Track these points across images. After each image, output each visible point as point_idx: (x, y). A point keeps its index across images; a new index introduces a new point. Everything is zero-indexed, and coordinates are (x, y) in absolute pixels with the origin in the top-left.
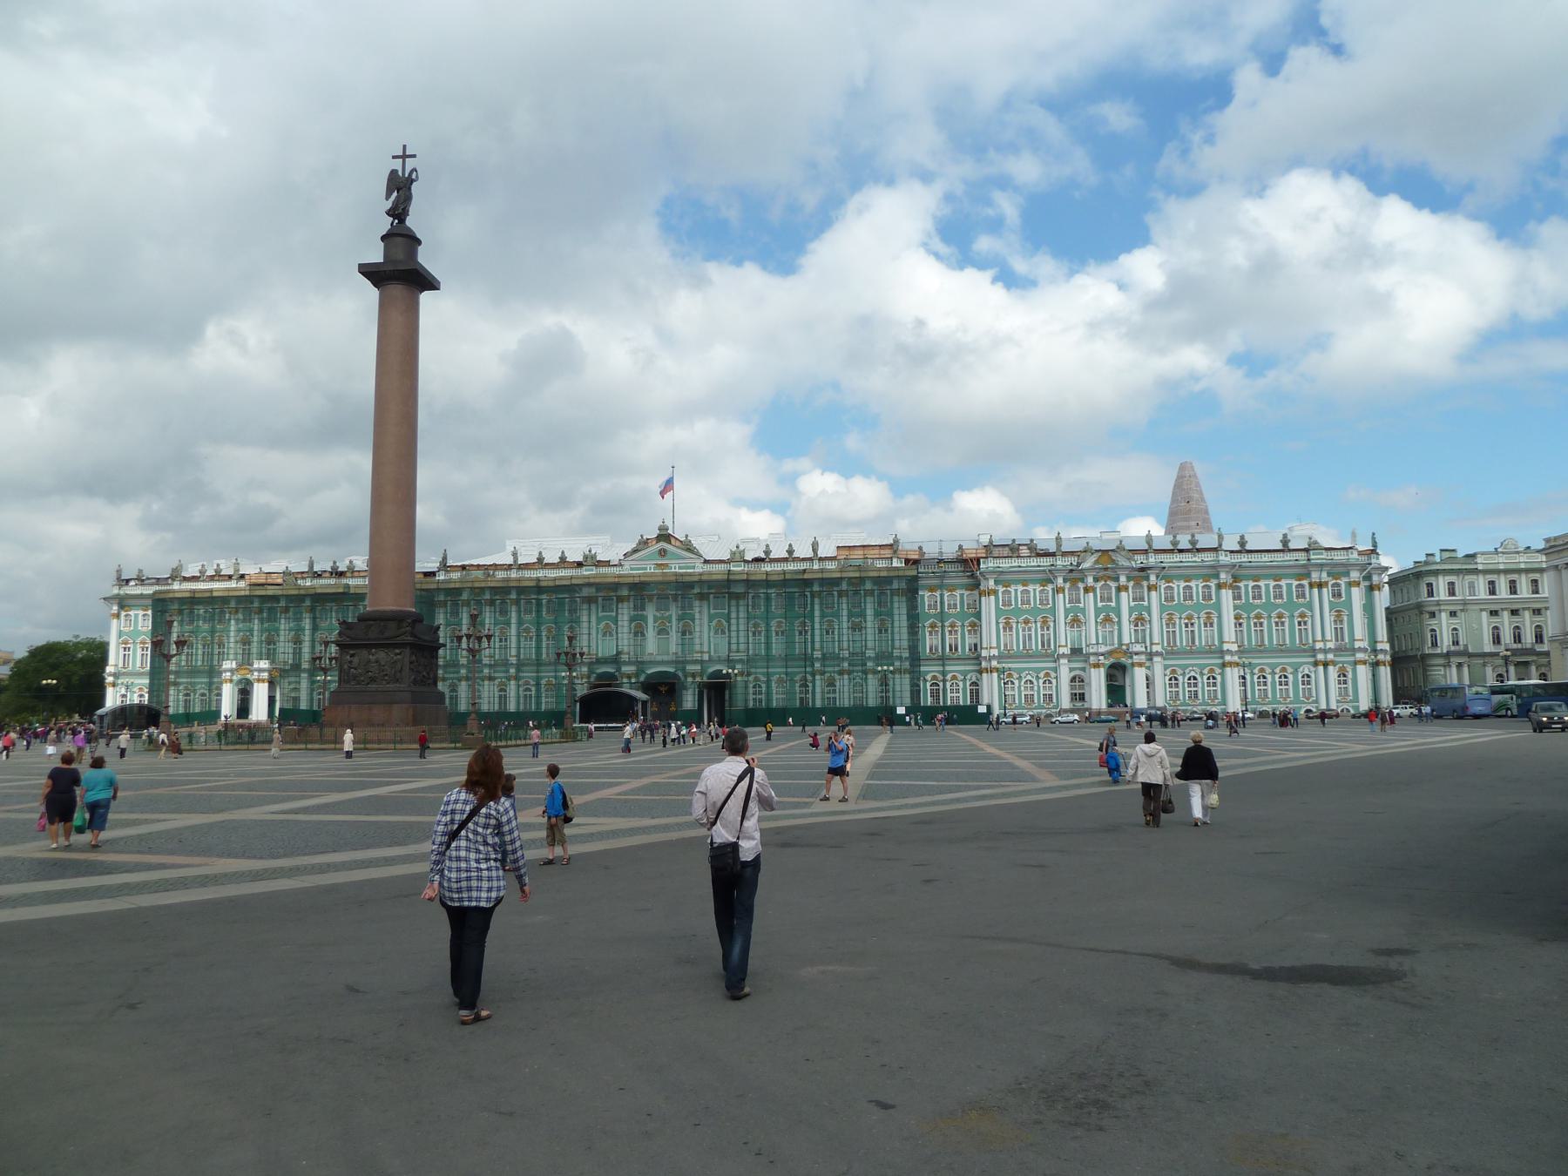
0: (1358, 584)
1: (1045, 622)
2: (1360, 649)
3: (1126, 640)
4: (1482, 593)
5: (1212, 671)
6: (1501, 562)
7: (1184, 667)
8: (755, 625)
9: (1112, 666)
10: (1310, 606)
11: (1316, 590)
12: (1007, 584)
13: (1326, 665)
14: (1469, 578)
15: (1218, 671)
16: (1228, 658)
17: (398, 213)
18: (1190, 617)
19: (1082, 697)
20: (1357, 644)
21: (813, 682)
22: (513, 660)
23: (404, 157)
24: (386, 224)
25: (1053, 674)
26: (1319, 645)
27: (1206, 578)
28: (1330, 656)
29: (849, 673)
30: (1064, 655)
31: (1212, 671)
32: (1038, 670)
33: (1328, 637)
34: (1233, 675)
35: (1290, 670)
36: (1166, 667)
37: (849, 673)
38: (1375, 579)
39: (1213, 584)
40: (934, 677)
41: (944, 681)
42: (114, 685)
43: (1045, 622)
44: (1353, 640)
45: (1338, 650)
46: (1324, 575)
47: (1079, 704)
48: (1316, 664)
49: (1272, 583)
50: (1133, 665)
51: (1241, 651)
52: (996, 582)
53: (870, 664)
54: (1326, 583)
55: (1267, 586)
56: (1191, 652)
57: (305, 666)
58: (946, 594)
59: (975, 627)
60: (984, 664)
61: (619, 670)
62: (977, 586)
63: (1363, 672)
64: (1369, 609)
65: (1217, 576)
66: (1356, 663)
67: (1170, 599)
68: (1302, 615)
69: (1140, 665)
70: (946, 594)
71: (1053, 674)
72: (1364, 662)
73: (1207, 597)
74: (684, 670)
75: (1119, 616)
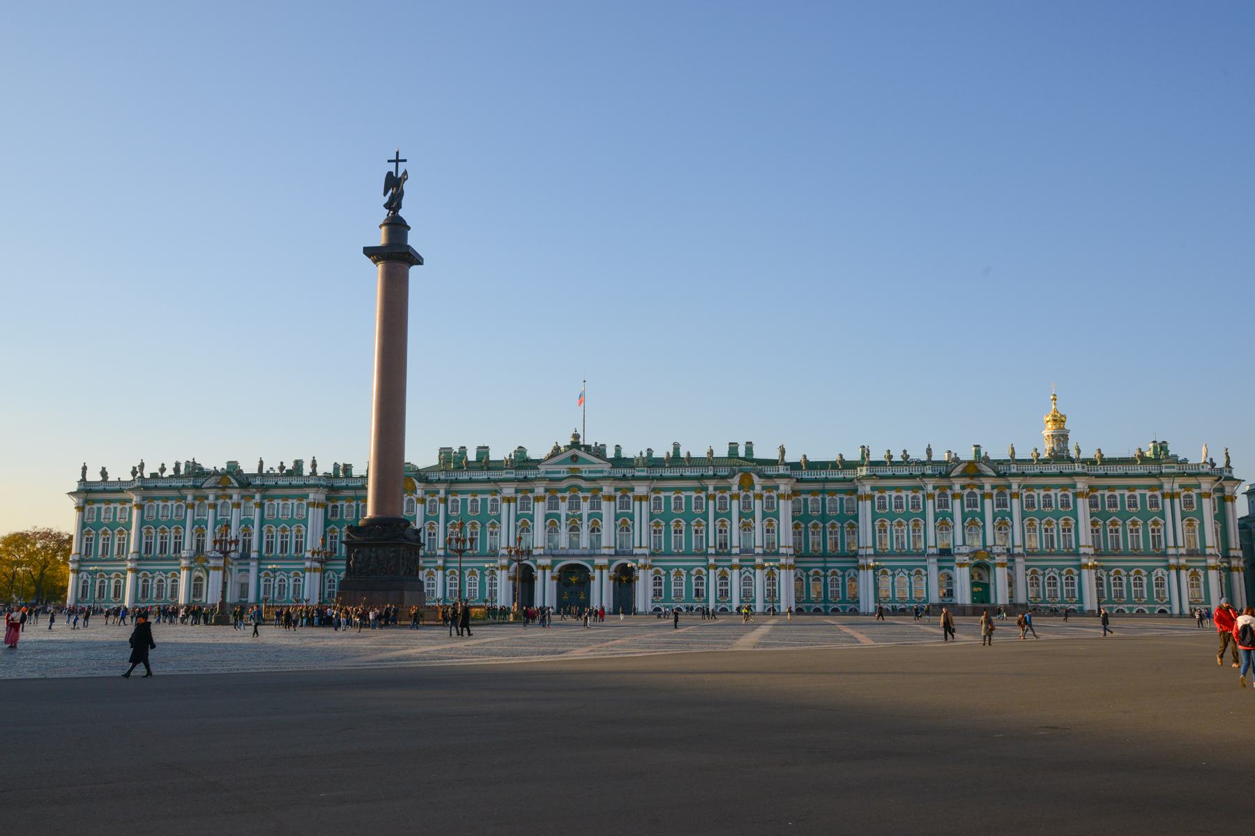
0: (1208, 495)
1: (916, 524)
2: (1211, 555)
3: (990, 542)
5: (1070, 572)
8: (657, 524)
9: (977, 566)
10: (1163, 516)
11: (1168, 501)
12: (882, 489)
13: (1178, 569)
15: (1076, 572)
16: (1084, 560)
17: (394, 204)
18: (1049, 523)
19: (950, 593)
20: (1208, 551)
22: (441, 552)
23: (397, 161)
24: (384, 214)
25: (924, 572)
26: (1171, 551)
28: (1182, 561)
29: (740, 568)
30: (933, 555)
31: (1070, 572)
32: (910, 568)
33: (1180, 543)
34: (1088, 578)
35: (1144, 573)
36: (1027, 568)
37: (740, 568)
38: (1228, 491)
39: (1070, 493)
40: (816, 573)
41: (826, 577)
43: (916, 524)
44: (1204, 546)
45: (1191, 553)
46: (1176, 486)
47: (947, 600)
48: (1168, 568)
49: (1127, 493)
50: (995, 565)
52: (873, 489)
54: (1178, 495)
55: (1122, 496)
56: (1050, 554)
57: (254, 555)
58: (828, 498)
59: (854, 528)
60: (862, 561)
61: (535, 562)
62: (855, 491)
63: (1213, 576)
64: (1221, 517)
65: (1074, 486)
66: (1206, 568)
68: (1155, 523)
69: (1003, 565)
71: (924, 572)
72: (1213, 568)
73: (1065, 504)
74: (592, 563)
75: (984, 521)
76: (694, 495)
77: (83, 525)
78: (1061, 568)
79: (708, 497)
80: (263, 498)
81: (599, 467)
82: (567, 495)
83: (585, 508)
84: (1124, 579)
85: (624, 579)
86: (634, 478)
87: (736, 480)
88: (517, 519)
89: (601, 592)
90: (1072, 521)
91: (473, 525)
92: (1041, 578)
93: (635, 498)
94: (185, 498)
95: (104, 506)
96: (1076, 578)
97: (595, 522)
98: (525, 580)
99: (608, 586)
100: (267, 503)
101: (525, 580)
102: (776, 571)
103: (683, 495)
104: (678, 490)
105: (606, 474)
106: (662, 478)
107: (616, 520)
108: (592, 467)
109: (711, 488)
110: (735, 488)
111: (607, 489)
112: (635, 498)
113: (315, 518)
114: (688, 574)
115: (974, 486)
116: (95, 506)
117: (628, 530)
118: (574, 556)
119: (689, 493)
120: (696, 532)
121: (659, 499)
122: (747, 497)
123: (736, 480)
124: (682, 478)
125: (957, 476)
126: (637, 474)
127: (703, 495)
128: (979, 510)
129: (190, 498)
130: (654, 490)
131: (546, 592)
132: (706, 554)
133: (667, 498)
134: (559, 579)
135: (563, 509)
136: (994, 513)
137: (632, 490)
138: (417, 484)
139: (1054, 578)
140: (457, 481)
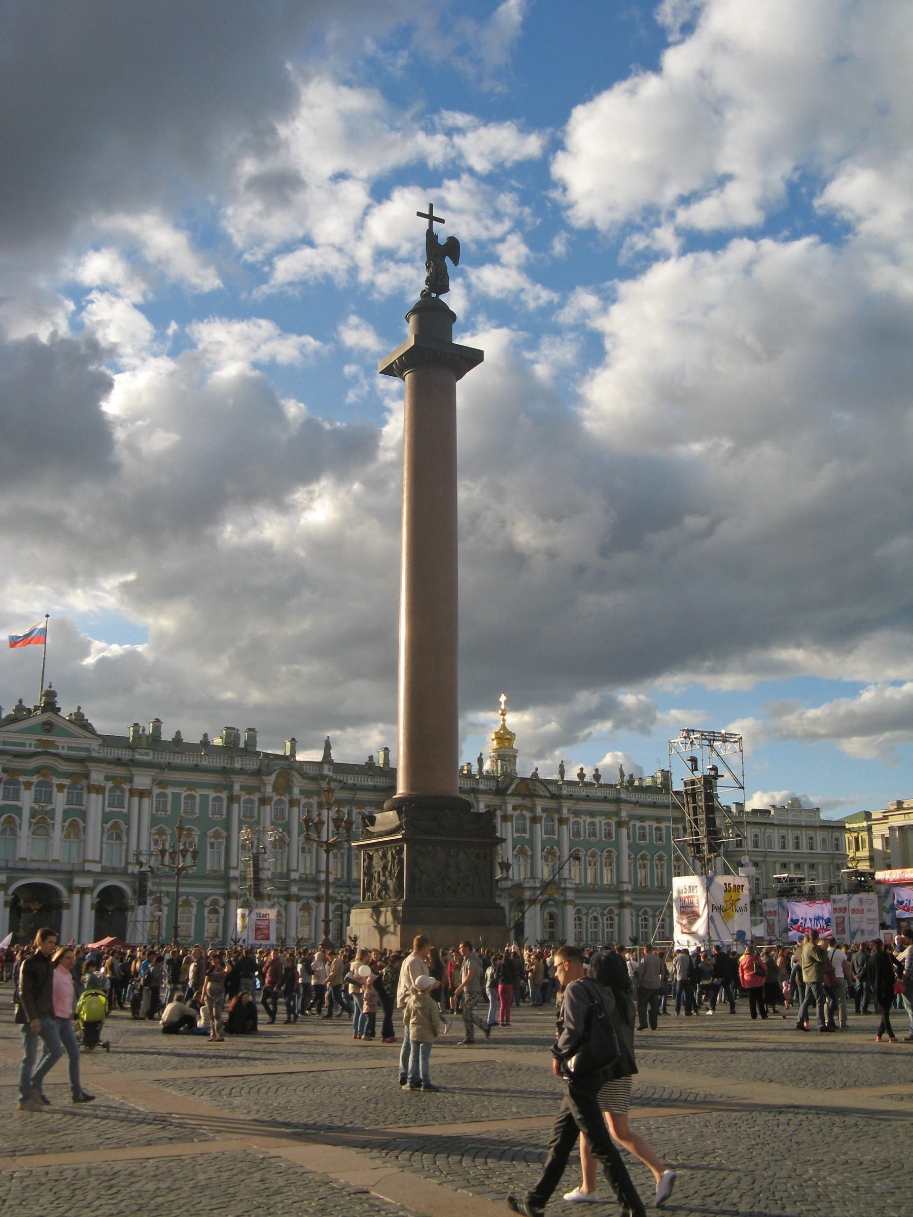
4: (777, 849)
6: (790, 819)
7: (589, 907)
8: (161, 832)
14: (769, 831)
15: (616, 911)
16: (627, 899)
18: (593, 855)
21: (226, 907)
27: (608, 815)
31: (611, 911)
49: (655, 825)
51: (636, 892)
53: (294, 889)
55: (651, 827)
56: (594, 891)
65: (617, 814)
67: (577, 834)
70: (355, 811)
73: (609, 835)
76: (212, 794)
78: (604, 907)
79: (232, 799)
81: (84, 743)
82: (35, 779)
83: (60, 801)
84: (651, 919)
86: (133, 763)
87: (273, 777)
90: (614, 855)
92: (584, 918)
93: (132, 793)
96: (616, 918)
97: (74, 824)
102: (313, 903)
103: (198, 793)
104: (191, 786)
105: (94, 754)
106: (170, 767)
107: (105, 821)
108: (74, 742)
109: (237, 787)
110: (269, 789)
111: (97, 777)
112: (132, 793)
114: (201, 905)
115: (526, 807)
117: (119, 838)
118: (38, 871)
119: (205, 792)
120: (212, 845)
121: (164, 795)
122: (280, 802)
123: (273, 777)
124: (196, 768)
125: (511, 795)
126: (137, 757)
127: (224, 795)
128: (527, 836)
130: (162, 784)
132: (226, 880)
133: (176, 796)
136: (543, 841)
137: (130, 780)
139: (596, 919)
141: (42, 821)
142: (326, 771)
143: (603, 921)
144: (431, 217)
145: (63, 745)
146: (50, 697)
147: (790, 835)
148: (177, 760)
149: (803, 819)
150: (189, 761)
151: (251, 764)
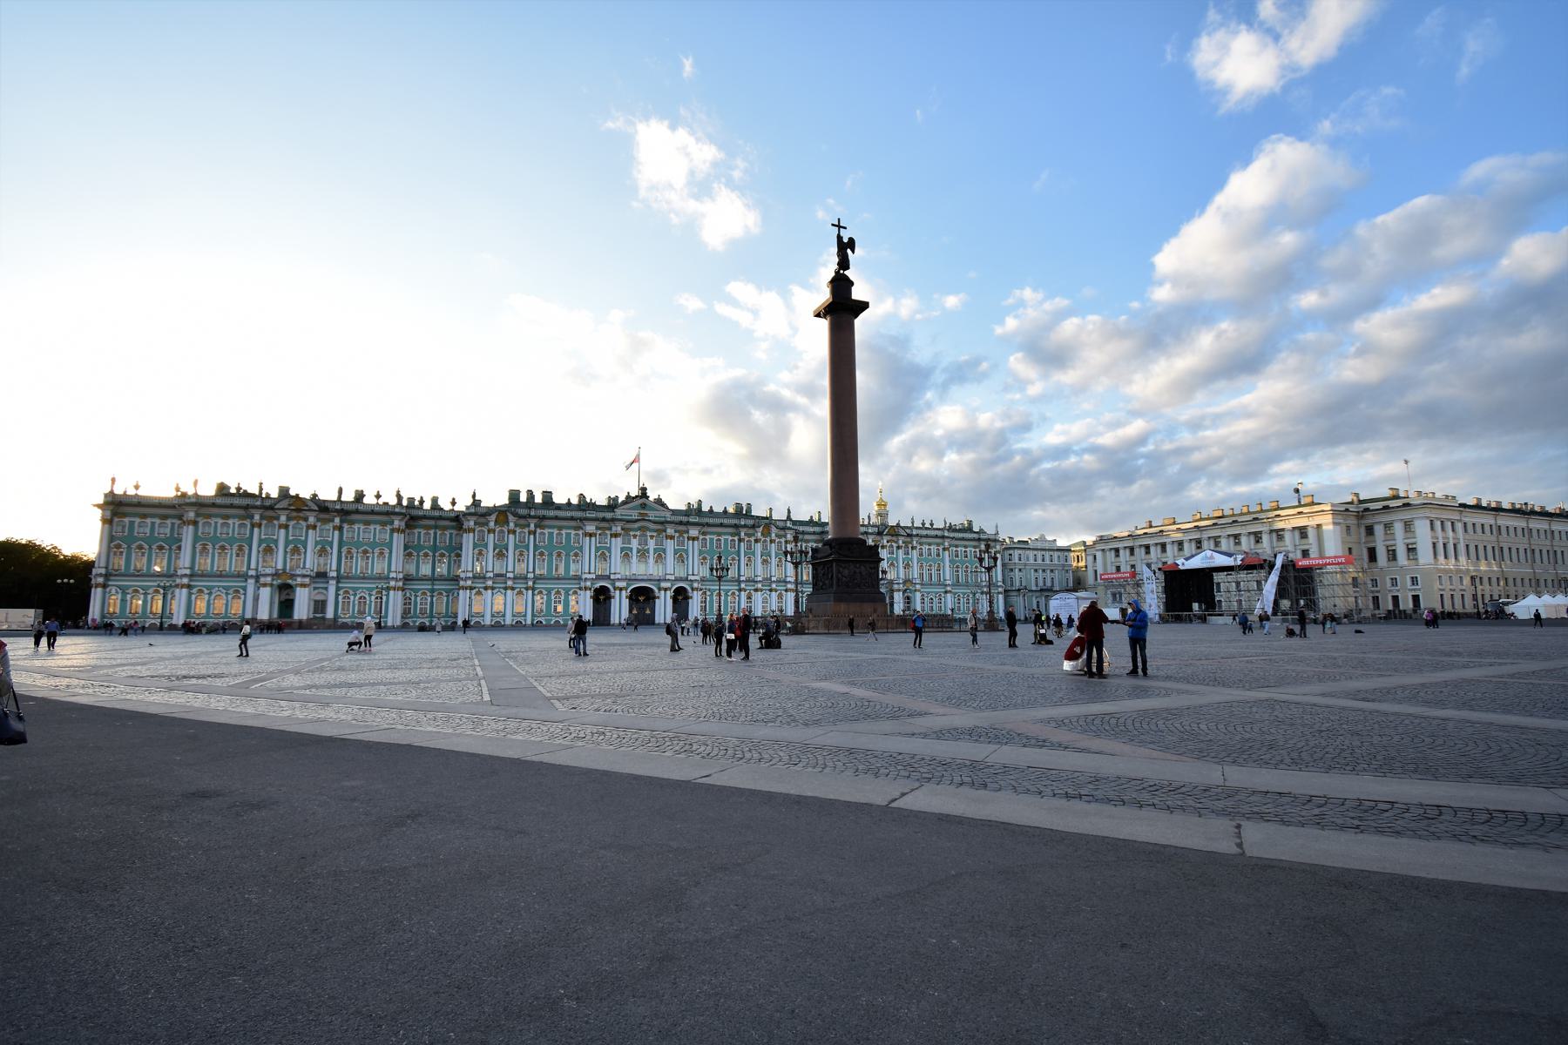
6: (1039, 545)
17: (844, 263)
22: (531, 575)
42: (104, 586)
77: (111, 538)
80: (342, 521)
83: (652, 544)
85: (681, 597)
86: (688, 523)
88: (597, 549)
89: (664, 610)
91: (559, 555)
94: (252, 517)
95: (137, 520)
98: (602, 597)
99: (670, 602)
100: (346, 526)
101: (602, 597)
104: (719, 534)
106: (708, 525)
111: (670, 531)
113: (398, 541)
116: (126, 520)
124: (721, 525)
129: (257, 518)
130: (704, 534)
131: (620, 608)
132: (739, 582)
134: (630, 598)
135: (635, 544)
138: (511, 517)
140: (544, 518)
141: (643, 554)
142: (789, 524)
143: (936, 600)
144: (839, 227)
145: (652, 515)
146: (644, 490)
147: (1039, 554)
148: (711, 521)
149: (1047, 546)
150: (718, 521)
151: (750, 522)
